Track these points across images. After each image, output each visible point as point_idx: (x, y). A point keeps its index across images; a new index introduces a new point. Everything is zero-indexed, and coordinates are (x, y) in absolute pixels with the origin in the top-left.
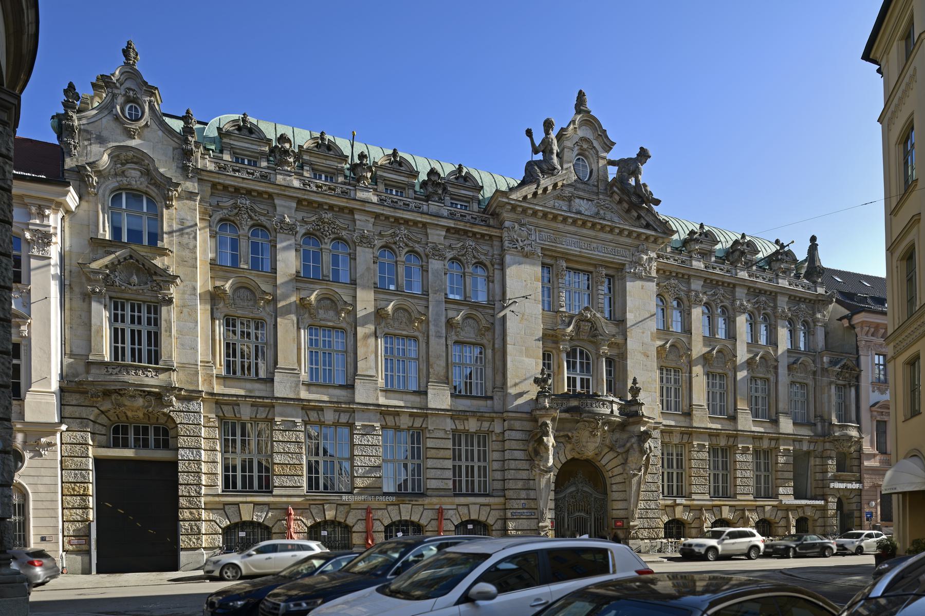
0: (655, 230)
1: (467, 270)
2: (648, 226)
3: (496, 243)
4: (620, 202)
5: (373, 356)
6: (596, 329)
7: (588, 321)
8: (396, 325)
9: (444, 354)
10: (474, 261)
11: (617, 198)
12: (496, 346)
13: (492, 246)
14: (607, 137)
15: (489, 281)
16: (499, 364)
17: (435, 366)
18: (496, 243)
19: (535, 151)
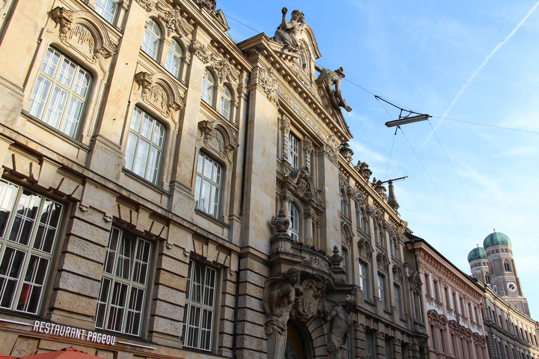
10: (226, 81)
17: (182, 165)
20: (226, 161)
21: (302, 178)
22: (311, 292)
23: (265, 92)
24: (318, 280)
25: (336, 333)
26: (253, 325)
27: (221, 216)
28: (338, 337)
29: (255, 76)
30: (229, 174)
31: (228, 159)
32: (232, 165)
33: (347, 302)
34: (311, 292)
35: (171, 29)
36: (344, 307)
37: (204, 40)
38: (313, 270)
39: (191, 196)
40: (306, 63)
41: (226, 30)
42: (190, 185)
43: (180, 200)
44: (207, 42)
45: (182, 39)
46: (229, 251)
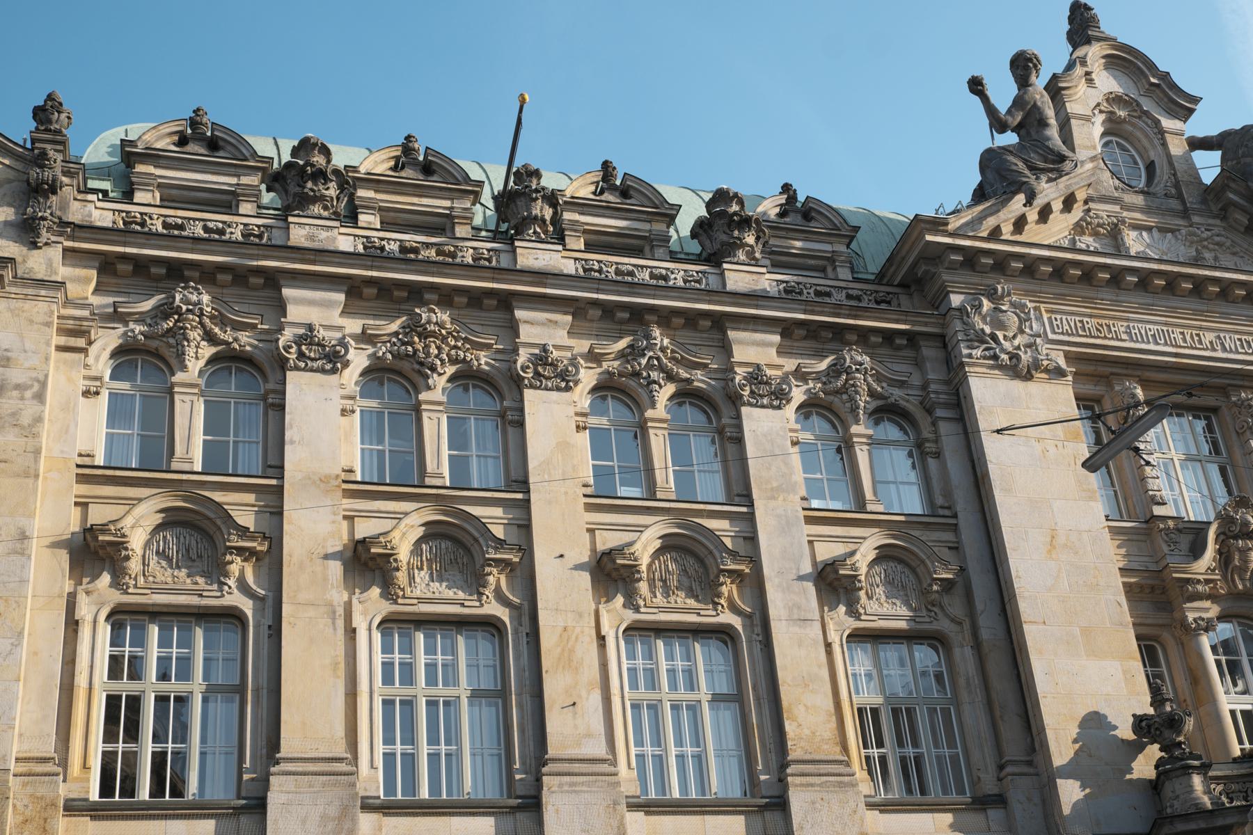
1: (854, 429)
3: (929, 352)
5: (596, 697)
8: (659, 600)
9: (825, 673)
12: (985, 634)
13: (918, 363)
14: (1174, 86)
15: (923, 455)
16: (1002, 686)
17: (799, 712)
18: (929, 352)
20: (944, 625)
21: (1236, 537)
27: (975, 779)
29: (955, 341)
30: (964, 656)
31: (947, 615)
32: (967, 626)
35: (655, 382)
39: (846, 779)
40: (1152, 155)
41: (852, 238)
42: (838, 749)
43: (813, 803)
44: (769, 345)
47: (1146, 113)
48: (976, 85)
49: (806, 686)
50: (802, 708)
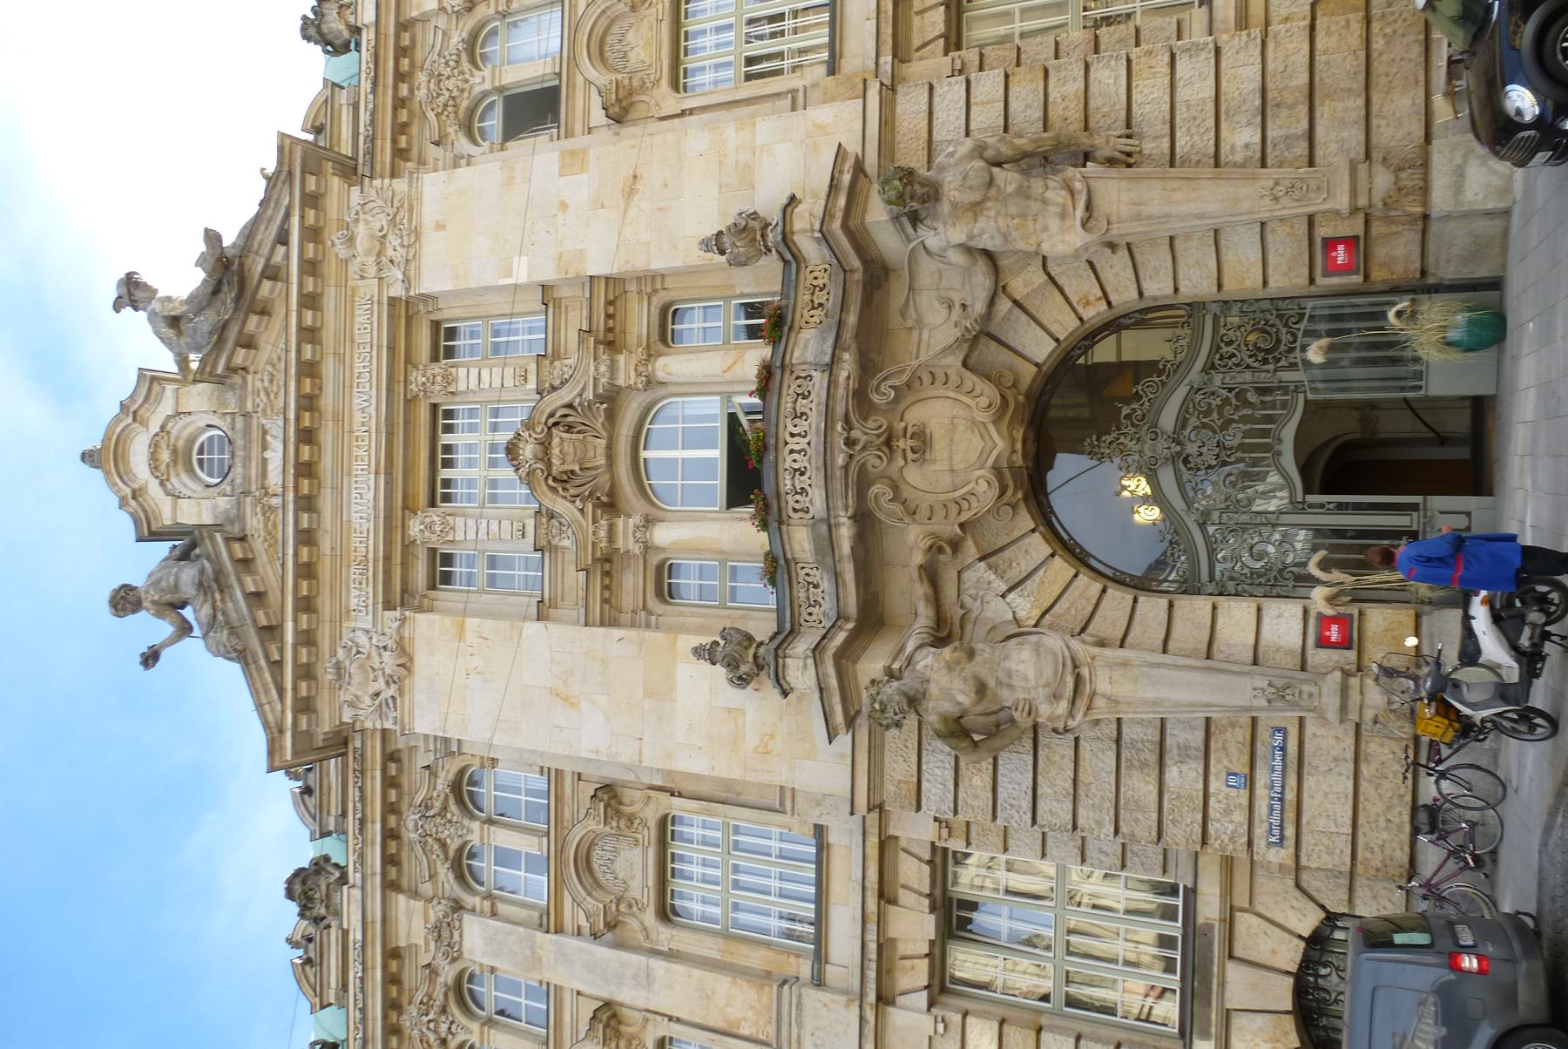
0: (287, 216)
2: (283, 239)
4: (249, 344)
6: (570, 406)
7: (545, 445)
11: (240, 356)
14: (132, 397)
19: (185, 629)
22: (913, 475)
23: (401, 691)
24: (863, 483)
25: (1033, 241)
26: (1081, 791)
28: (1046, 229)
33: (896, 219)
34: (913, 475)
36: (915, 219)
37: (410, 916)
38: (838, 525)
45: (450, 981)
46: (886, 844)
47: (163, 428)
48: (150, 658)
49: (707, 997)
50: (729, 1010)
